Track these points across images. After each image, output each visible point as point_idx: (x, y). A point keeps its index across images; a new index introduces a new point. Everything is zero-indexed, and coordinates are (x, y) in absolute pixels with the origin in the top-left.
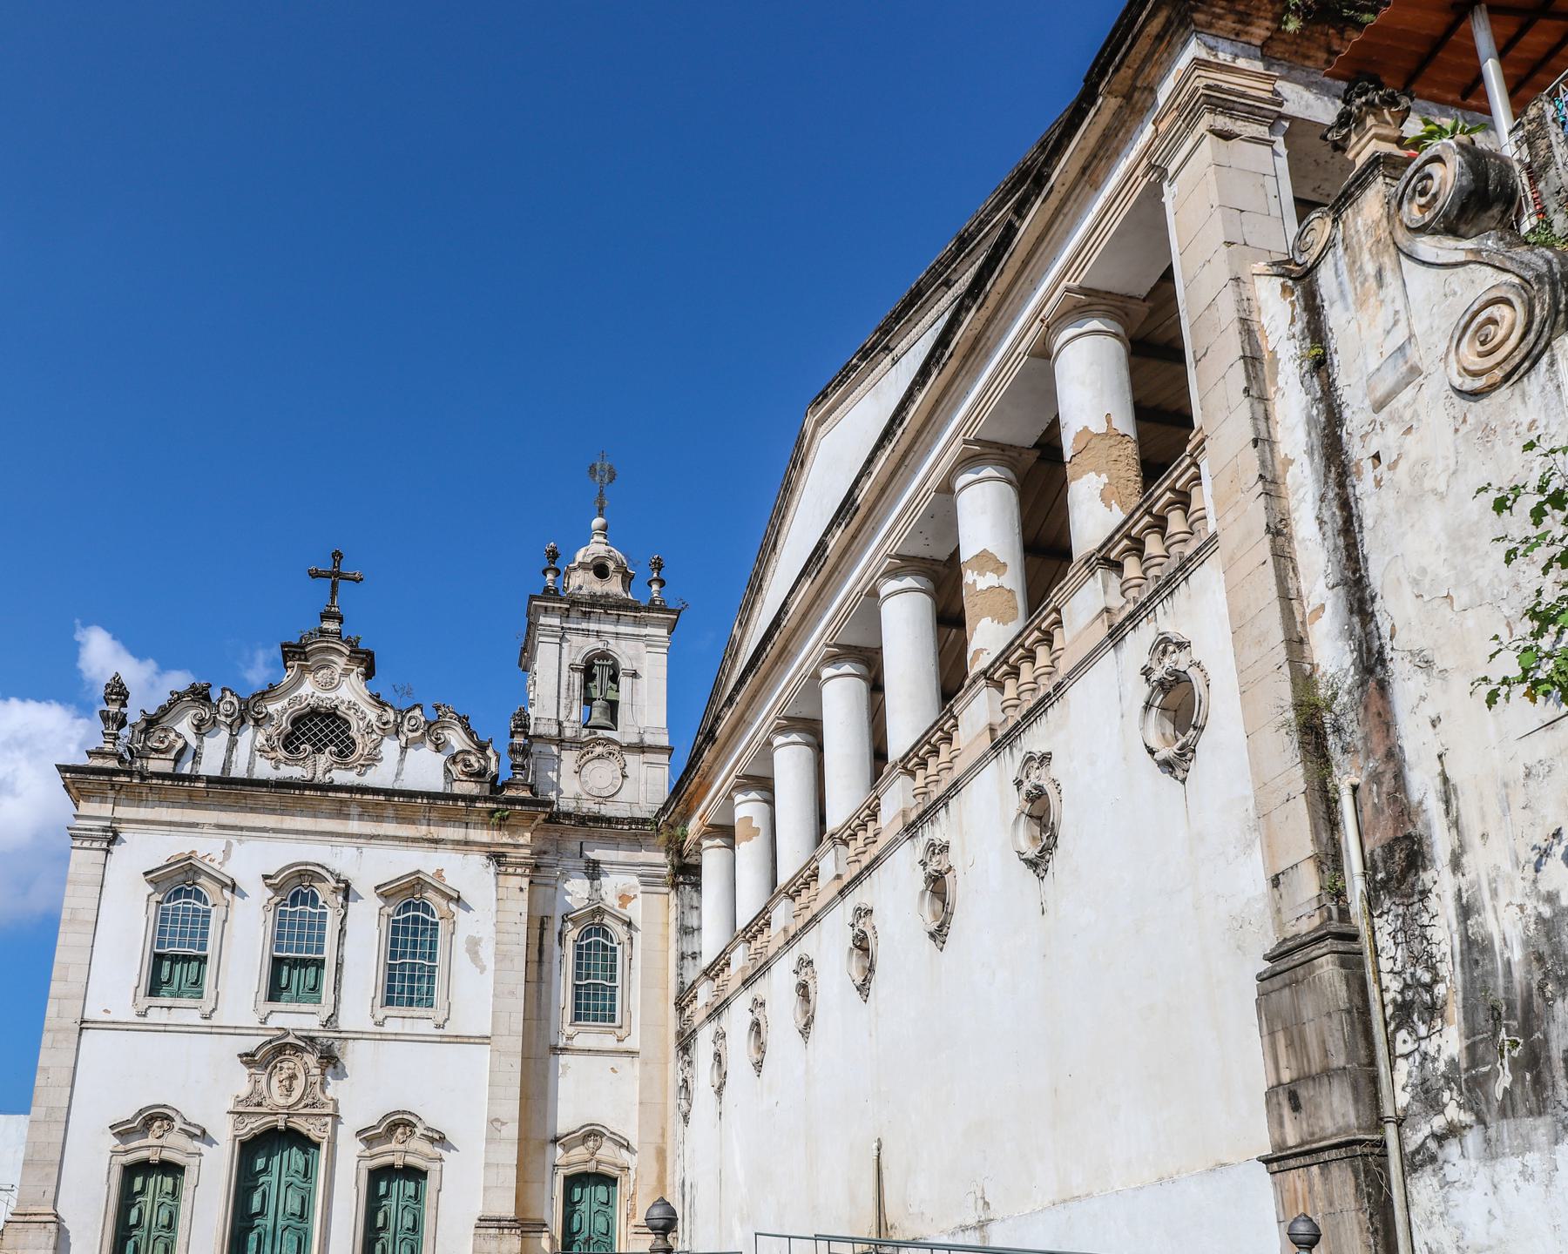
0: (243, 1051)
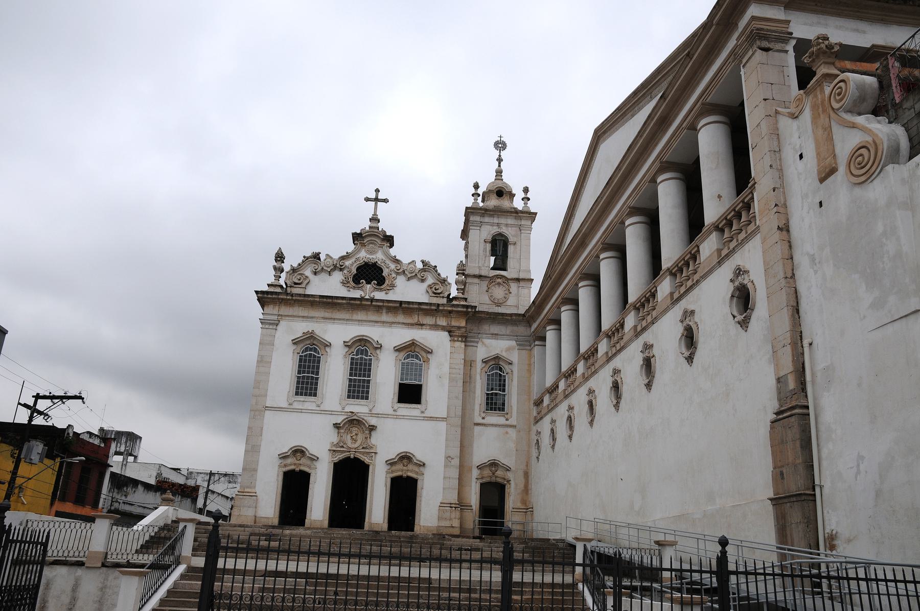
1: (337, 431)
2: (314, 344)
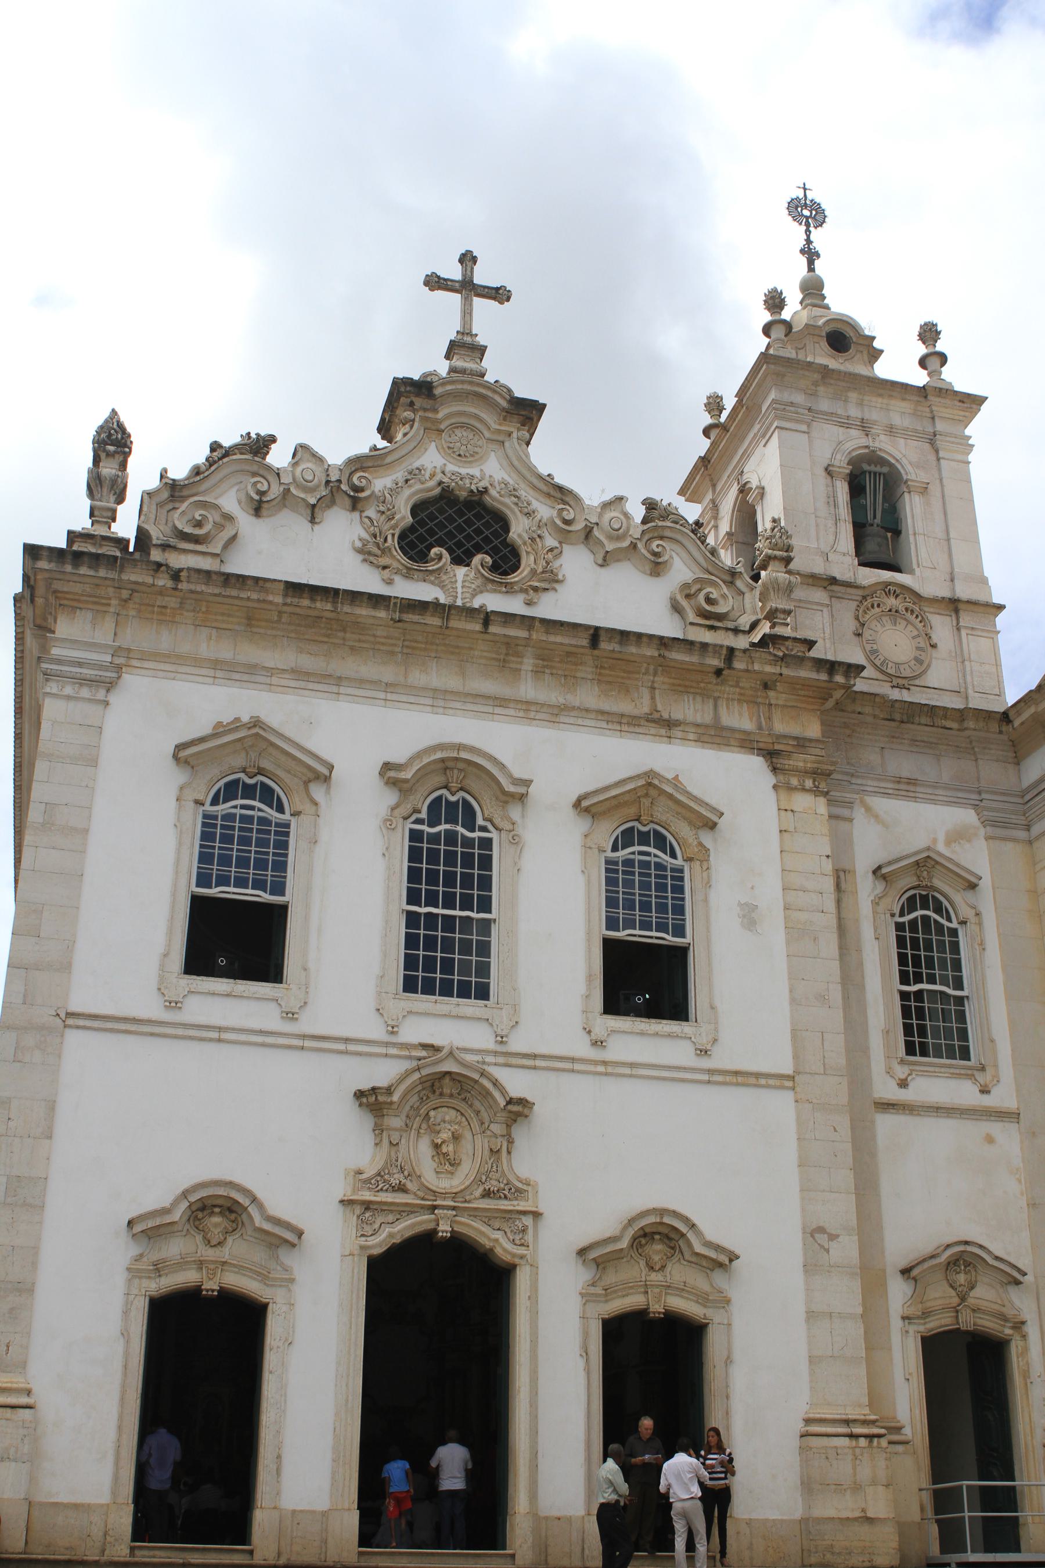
0: (365, 1086)
1: (367, 1121)
2: (261, 772)
